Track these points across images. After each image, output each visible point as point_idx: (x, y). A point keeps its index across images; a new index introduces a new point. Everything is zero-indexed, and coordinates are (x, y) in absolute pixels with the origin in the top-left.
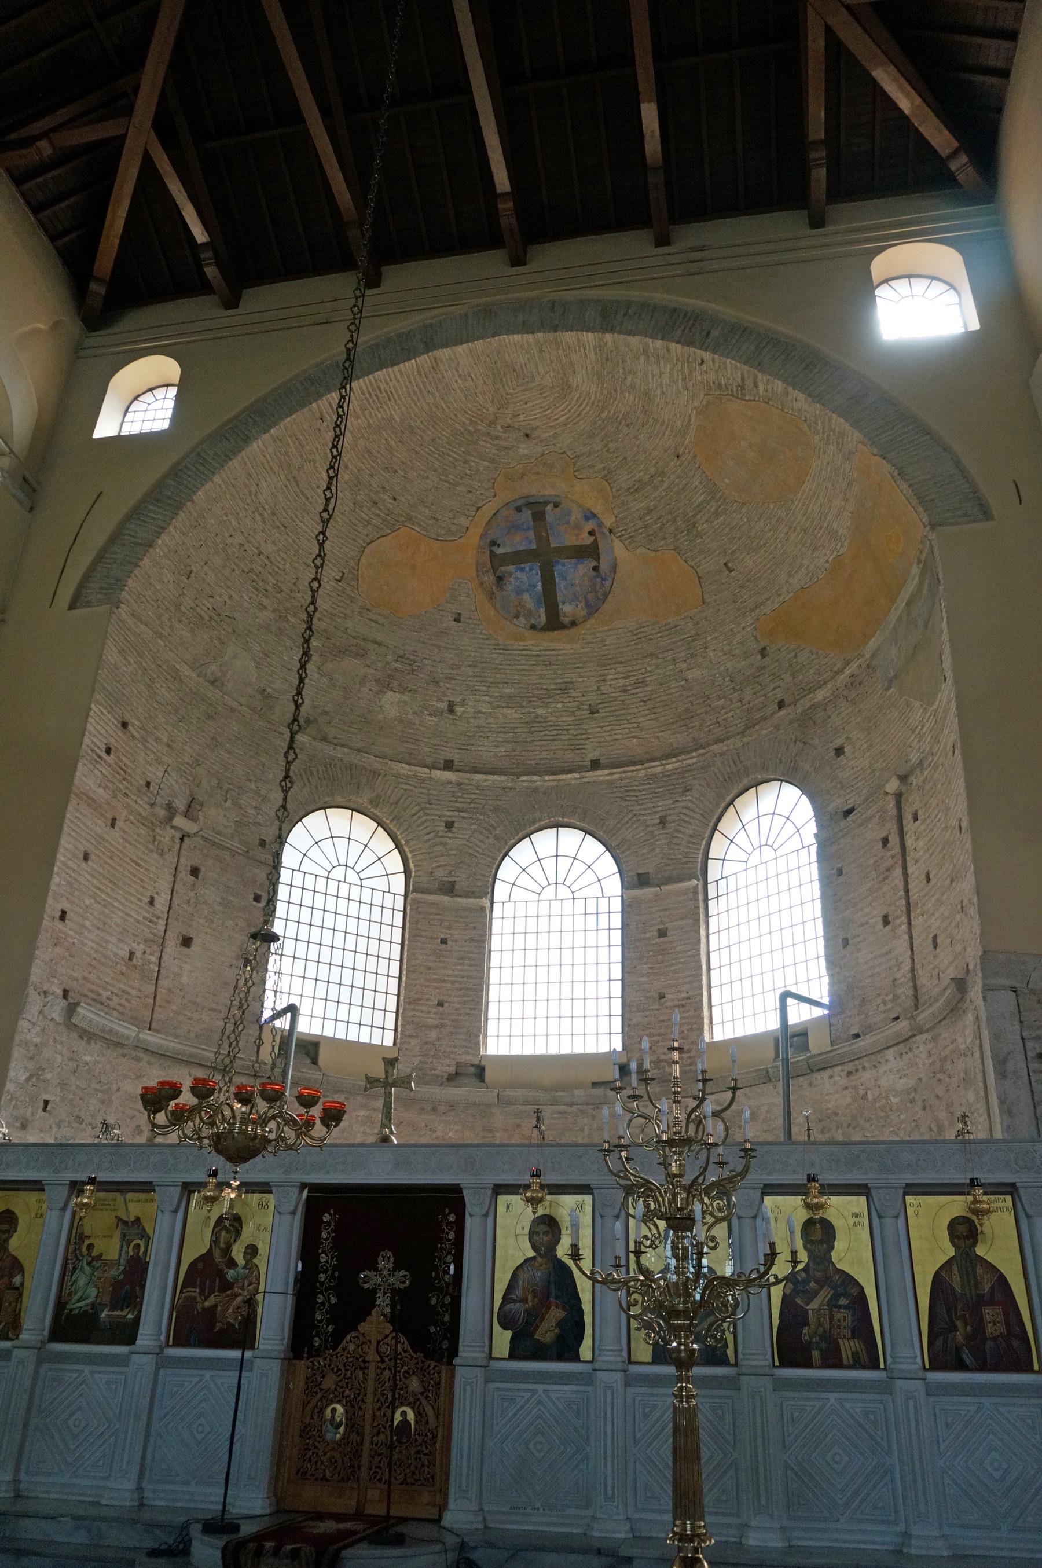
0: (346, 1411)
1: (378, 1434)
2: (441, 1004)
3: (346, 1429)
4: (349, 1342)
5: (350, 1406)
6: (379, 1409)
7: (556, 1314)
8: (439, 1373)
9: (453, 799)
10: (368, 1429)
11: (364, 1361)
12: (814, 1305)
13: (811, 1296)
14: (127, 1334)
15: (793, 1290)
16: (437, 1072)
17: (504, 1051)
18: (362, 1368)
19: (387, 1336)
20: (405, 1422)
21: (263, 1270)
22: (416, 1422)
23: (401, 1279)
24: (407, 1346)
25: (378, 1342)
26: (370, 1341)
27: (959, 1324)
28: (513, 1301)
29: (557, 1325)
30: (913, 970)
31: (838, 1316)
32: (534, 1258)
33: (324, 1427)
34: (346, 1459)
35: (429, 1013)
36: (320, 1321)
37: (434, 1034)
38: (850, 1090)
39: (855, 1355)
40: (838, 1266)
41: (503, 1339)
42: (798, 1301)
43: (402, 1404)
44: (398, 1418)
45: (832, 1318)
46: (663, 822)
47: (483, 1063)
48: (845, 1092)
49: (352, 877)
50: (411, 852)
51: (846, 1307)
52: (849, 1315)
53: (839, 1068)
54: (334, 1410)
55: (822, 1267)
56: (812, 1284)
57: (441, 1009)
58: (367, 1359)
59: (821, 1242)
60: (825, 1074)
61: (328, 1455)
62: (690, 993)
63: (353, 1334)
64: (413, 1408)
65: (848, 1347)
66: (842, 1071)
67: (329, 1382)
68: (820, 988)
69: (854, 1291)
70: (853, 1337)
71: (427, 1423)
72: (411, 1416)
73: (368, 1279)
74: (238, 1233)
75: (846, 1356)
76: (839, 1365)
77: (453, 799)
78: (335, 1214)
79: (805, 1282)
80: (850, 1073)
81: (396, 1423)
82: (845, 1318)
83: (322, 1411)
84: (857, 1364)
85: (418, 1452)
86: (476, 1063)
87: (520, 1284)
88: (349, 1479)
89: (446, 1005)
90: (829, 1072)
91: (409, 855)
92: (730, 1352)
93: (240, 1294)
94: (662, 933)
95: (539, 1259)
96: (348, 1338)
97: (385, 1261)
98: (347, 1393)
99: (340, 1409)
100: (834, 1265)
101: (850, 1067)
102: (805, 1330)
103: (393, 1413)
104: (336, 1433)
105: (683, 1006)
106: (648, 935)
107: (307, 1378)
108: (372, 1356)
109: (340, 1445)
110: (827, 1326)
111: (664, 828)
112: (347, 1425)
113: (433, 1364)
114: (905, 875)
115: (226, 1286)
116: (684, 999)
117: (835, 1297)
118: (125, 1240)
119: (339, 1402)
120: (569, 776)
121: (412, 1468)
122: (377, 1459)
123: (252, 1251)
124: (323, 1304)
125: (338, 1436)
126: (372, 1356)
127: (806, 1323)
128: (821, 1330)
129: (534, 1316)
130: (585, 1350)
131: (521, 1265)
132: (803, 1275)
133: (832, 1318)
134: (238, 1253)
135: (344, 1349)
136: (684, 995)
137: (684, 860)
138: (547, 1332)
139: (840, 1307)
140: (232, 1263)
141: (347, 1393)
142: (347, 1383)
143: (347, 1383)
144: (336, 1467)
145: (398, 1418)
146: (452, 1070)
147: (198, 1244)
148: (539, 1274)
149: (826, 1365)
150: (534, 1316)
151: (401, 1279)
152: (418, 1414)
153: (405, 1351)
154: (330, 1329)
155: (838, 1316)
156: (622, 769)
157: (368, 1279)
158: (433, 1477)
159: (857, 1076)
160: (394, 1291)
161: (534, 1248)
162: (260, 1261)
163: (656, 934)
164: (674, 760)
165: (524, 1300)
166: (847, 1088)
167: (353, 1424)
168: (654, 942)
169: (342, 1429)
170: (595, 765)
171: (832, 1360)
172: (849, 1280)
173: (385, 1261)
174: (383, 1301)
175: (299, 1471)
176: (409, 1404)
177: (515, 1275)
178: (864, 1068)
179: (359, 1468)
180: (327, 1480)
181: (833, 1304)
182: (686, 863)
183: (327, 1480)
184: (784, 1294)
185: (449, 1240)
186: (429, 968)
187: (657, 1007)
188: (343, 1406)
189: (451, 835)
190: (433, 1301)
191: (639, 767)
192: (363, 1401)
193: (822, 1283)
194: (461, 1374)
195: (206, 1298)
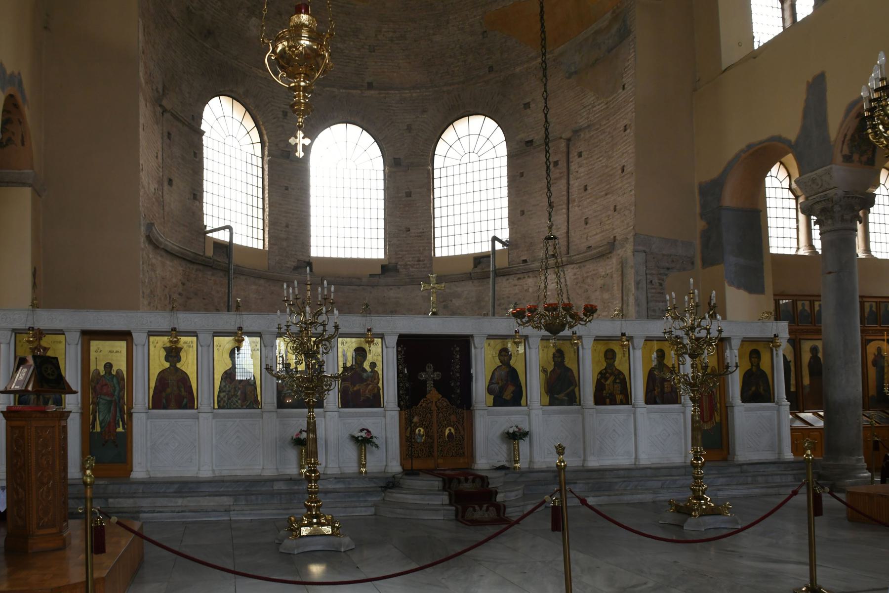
0: (425, 430)
1: (440, 438)
2: (287, 226)
3: (425, 438)
5: (425, 428)
6: (439, 429)
7: (511, 389)
8: (463, 413)
9: (287, 97)
10: (436, 437)
11: (430, 410)
12: (608, 382)
13: (606, 379)
15: (600, 377)
16: (288, 265)
17: (321, 255)
18: (430, 413)
19: (439, 400)
20: (450, 433)
21: (380, 373)
22: (455, 433)
23: (436, 375)
24: (449, 403)
25: (436, 402)
26: (432, 402)
27: (656, 388)
28: (493, 383)
29: (512, 393)
30: (568, 232)
31: (616, 386)
32: (500, 366)
33: (416, 437)
34: (427, 449)
35: (282, 231)
36: (402, 394)
37: (285, 244)
38: (518, 286)
39: (621, 400)
40: (617, 368)
42: (602, 381)
43: (448, 426)
44: (447, 432)
45: (614, 387)
46: (409, 128)
47: (311, 261)
48: (515, 287)
49: (236, 144)
50: (266, 130)
51: (618, 383)
52: (619, 385)
53: (513, 276)
54: (420, 431)
55: (611, 368)
56: (607, 375)
57: (288, 229)
58: (432, 409)
59: (612, 358)
60: (504, 279)
61: (420, 448)
62: (425, 230)
63: (425, 399)
64: (453, 428)
65: (619, 397)
66: (515, 277)
67: (416, 419)
68: (505, 235)
69: (622, 377)
70: (621, 394)
71: (460, 433)
72: (453, 431)
74: (365, 357)
75: (618, 401)
76: (616, 404)
77: (287, 97)
78: (403, 347)
79: (605, 374)
80: (519, 279)
81: (446, 434)
82: (618, 387)
83: (414, 431)
84: (622, 403)
85: (457, 444)
86: (307, 260)
87: (496, 376)
88: (429, 456)
89: (290, 227)
90: (507, 277)
91: (264, 132)
92: (578, 400)
93: (371, 384)
94: (409, 194)
95: (503, 367)
96: (422, 401)
97: (430, 368)
98: (424, 423)
99: (422, 430)
100: (615, 367)
101: (518, 276)
102: (604, 392)
103: (445, 430)
104: (422, 439)
105: (420, 236)
106: (400, 195)
107: (406, 418)
108: (434, 408)
109: (424, 444)
110: (612, 390)
111: (410, 132)
112: (426, 436)
113: (460, 410)
114: (568, 184)
115: (362, 380)
116: (421, 233)
117: (615, 379)
119: (421, 427)
120: (355, 91)
121: (455, 450)
122: (440, 448)
123: (373, 365)
124: (403, 387)
125: (423, 440)
126: (434, 408)
127: (605, 390)
128: (610, 392)
129: (502, 390)
131: (496, 369)
132: (604, 371)
133: (614, 387)
134: (366, 365)
135: (421, 406)
136: (421, 230)
137: (421, 153)
138: (508, 395)
139: (616, 383)
140: (365, 370)
141: (424, 423)
142: (424, 420)
143: (424, 420)
144: (423, 452)
145: (447, 432)
146: (295, 264)
148: (503, 373)
149: (611, 404)
150: (502, 390)
151: (436, 375)
152: (455, 430)
153: (448, 405)
154: (407, 397)
155: (616, 386)
156: (386, 92)
158: (464, 453)
159: (524, 280)
160: (434, 381)
161: (501, 362)
162: (378, 369)
163: (404, 195)
164: (418, 91)
165: (498, 383)
166: (516, 285)
167: (427, 434)
168: (403, 199)
169: (424, 438)
170: (370, 86)
171: (613, 402)
172: (620, 373)
173: (430, 368)
174: (430, 385)
175: (407, 455)
176: (452, 426)
177: (493, 373)
178: (529, 277)
179: (433, 452)
180: (420, 457)
181: (614, 382)
182: (423, 155)
183: (420, 457)
184: (597, 379)
185: (457, 359)
186: (280, 204)
187: (404, 236)
188: (424, 428)
189: (286, 121)
190: (452, 385)
191: (397, 92)
192: (432, 426)
193: (611, 374)
195: (355, 386)
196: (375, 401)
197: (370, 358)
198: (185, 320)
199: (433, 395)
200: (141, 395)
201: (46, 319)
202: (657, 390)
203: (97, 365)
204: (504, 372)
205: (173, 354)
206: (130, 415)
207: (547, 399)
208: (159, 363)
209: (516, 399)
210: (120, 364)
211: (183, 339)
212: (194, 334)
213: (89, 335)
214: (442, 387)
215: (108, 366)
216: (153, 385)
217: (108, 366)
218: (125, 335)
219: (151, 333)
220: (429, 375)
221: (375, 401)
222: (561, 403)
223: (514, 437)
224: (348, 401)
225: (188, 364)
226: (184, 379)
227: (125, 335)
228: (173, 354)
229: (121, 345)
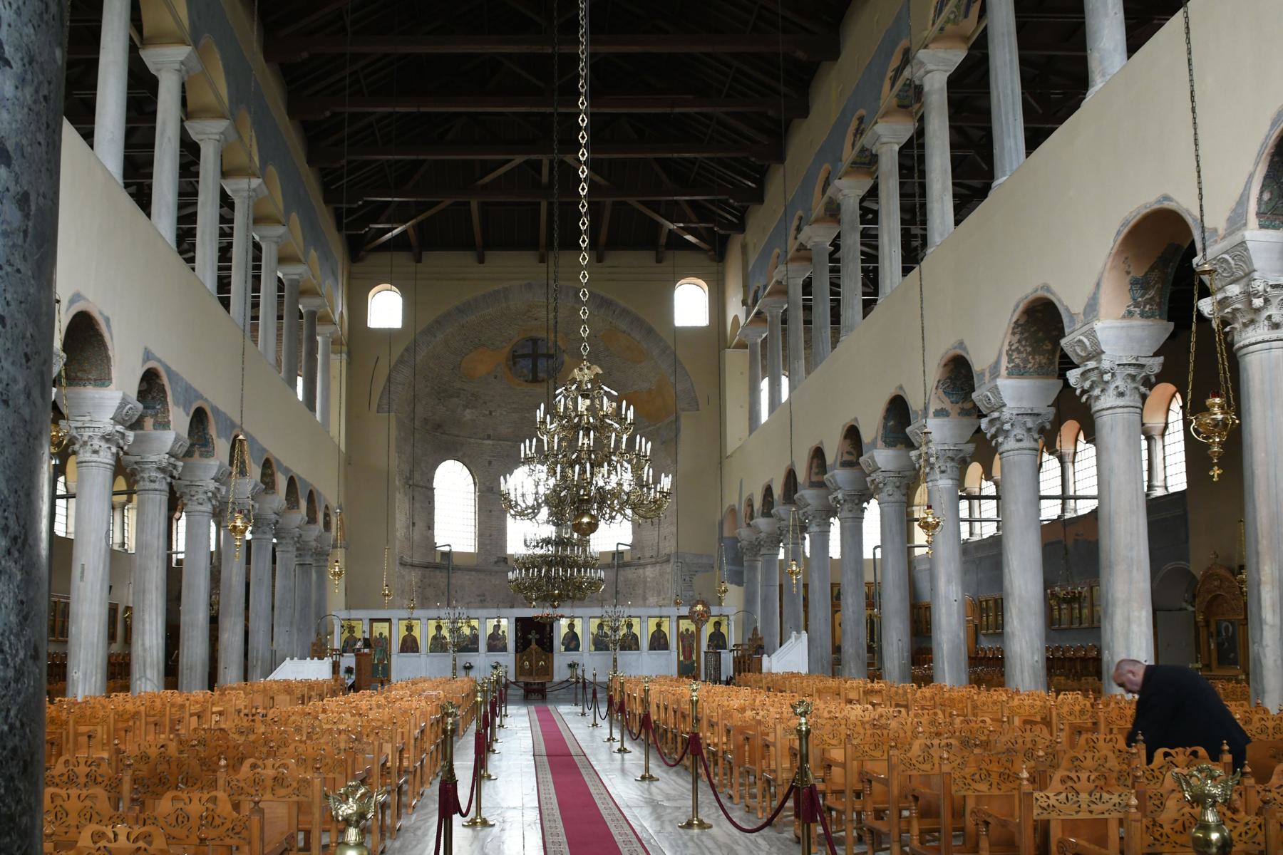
4: (528, 650)
14: (476, 650)
23: (537, 636)
41: (563, 648)
65: (633, 647)
67: (525, 657)
73: (530, 636)
82: (633, 642)
84: (635, 650)
108: (534, 652)
115: (498, 639)
118: (472, 630)
123: (503, 632)
126: (534, 652)
129: (569, 643)
130: (580, 649)
134: (500, 632)
138: (572, 646)
147: (490, 630)
150: (569, 643)
151: (537, 636)
157: (530, 636)
167: (530, 665)
194: (555, 655)
196: (504, 649)
197: (502, 629)
198: (417, 613)
199: (534, 646)
200: (395, 646)
201: (355, 614)
202: (656, 643)
203: (376, 634)
204: (570, 635)
205: (410, 628)
206: (390, 656)
207: (593, 648)
208: (404, 632)
209: (576, 648)
210: (386, 633)
211: (414, 622)
212: (419, 619)
213: (372, 620)
214: (539, 642)
215: (381, 634)
216: (400, 642)
217: (381, 634)
218: (388, 620)
219: (400, 619)
220: (533, 636)
221: (504, 649)
222: (601, 650)
223: (572, 666)
224: (491, 648)
225: (416, 633)
226: (414, 640)
227: (388, 620)
228: (410, 628)
229: (387, 624)
